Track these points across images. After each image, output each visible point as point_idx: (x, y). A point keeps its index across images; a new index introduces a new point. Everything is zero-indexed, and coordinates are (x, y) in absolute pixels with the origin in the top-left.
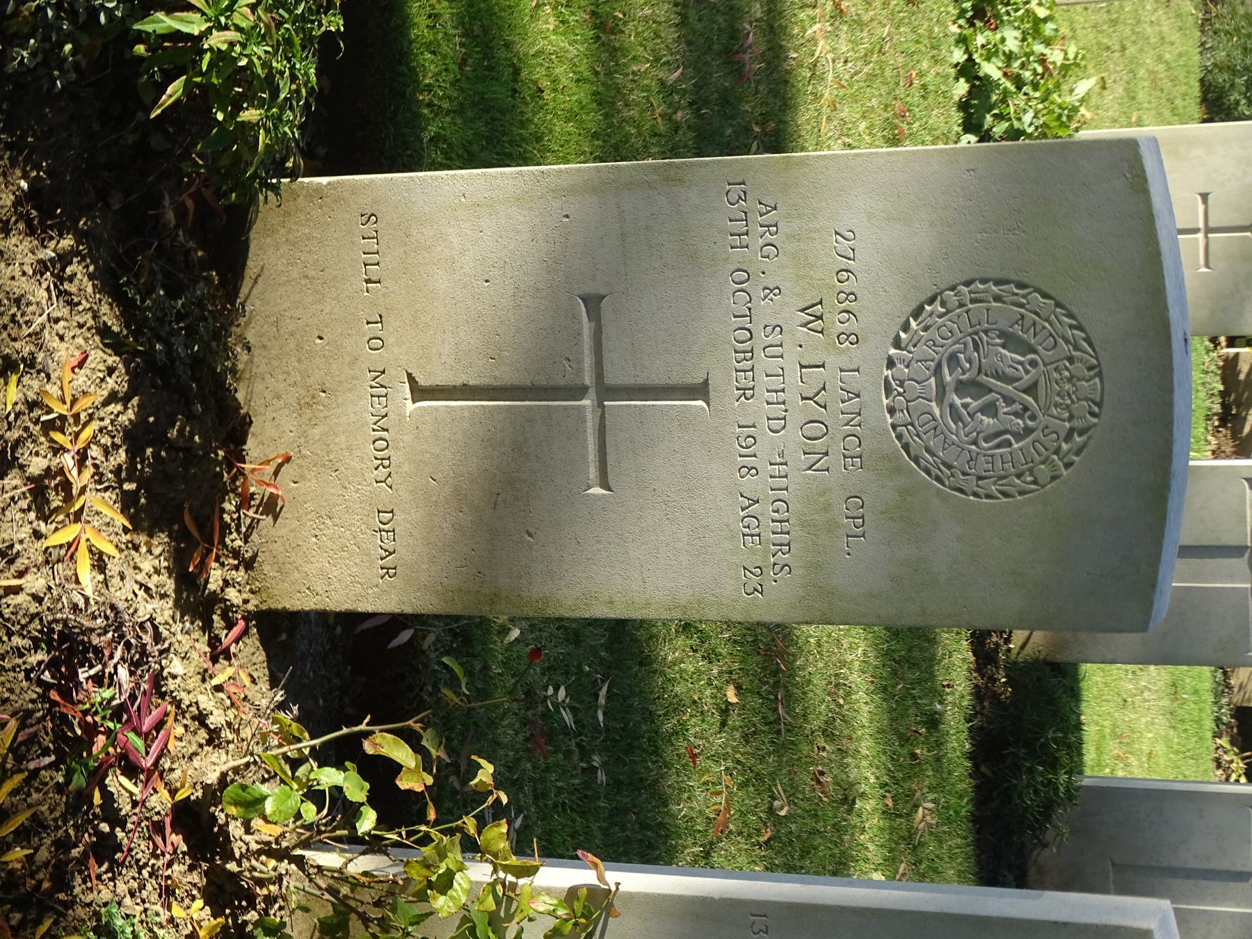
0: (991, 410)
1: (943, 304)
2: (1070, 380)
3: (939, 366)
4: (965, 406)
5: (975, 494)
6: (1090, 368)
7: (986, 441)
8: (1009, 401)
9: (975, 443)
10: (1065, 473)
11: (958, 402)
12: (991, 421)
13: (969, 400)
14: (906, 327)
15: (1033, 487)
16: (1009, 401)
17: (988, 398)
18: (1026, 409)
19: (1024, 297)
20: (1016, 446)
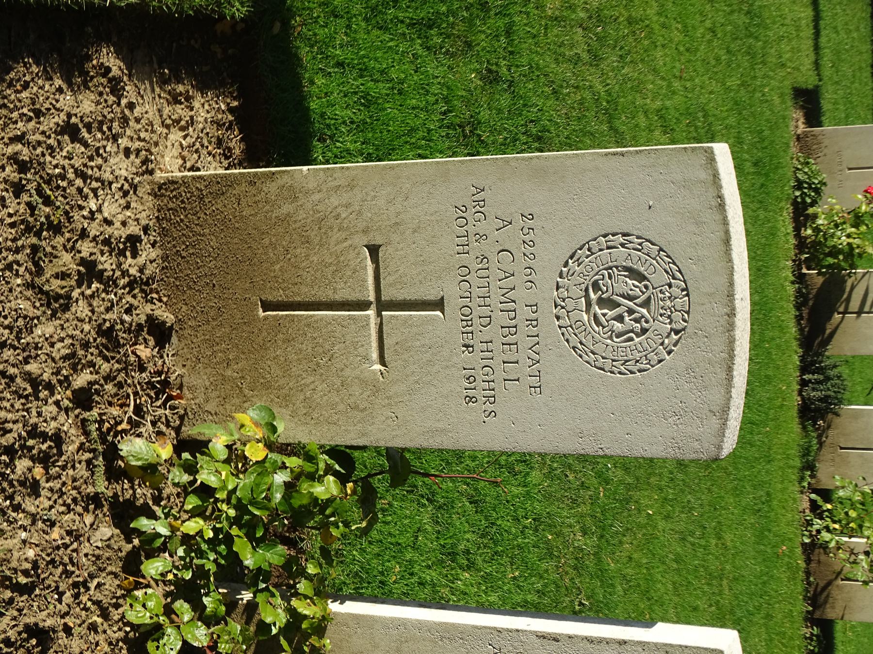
0: (620, 318)
1: (589, 250)
2: (669, 298)
3: (587, 290)
4: (604, 315)
5: (612, 372)
6: (683, 290)
7: (617, 337)
8: (631, 312)
9: (611, 338)
10: (667, 357)
11: (599, 311)
12: (619, 325)
13: (605, 311)
14: (566, 264)
15: (648, 366)
16: (631, 312)
17: (618, 311)
18: (643, 317)
19: (640, 244)
20: (637, 340)
